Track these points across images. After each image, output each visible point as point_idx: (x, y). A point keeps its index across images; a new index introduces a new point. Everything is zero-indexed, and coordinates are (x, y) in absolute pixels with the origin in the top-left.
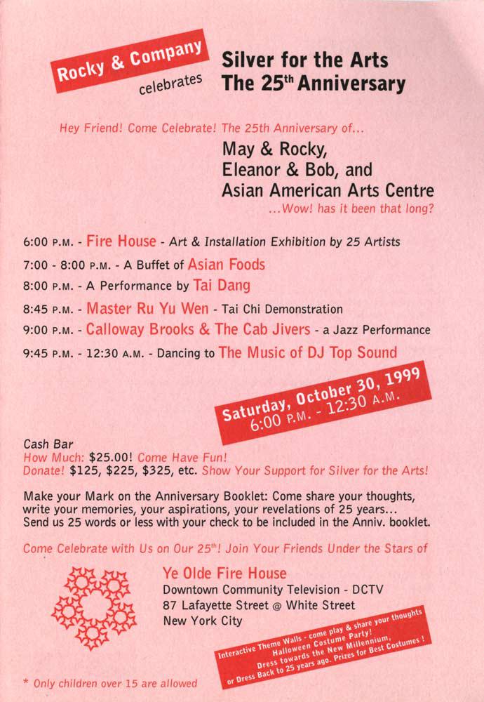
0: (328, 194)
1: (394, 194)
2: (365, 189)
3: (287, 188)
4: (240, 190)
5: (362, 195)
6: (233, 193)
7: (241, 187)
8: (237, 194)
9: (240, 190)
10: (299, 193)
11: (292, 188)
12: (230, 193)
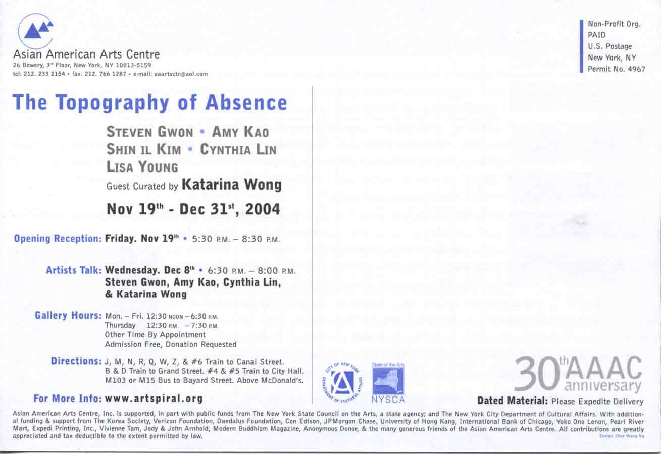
0: (86, 56)
1: (132, 57)
2: (112, 53)
3: (58, 52)
4: (26, 54)
5: (110, 57)
6: (22, 56)
7: (27, 52)
8: (24, 56)
9: (26, 54)
10: (67, 56)
11: (62, 53)
12: (19, 55)
